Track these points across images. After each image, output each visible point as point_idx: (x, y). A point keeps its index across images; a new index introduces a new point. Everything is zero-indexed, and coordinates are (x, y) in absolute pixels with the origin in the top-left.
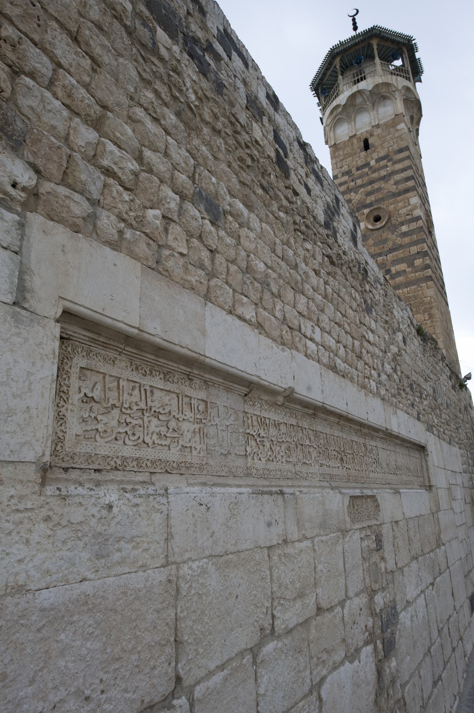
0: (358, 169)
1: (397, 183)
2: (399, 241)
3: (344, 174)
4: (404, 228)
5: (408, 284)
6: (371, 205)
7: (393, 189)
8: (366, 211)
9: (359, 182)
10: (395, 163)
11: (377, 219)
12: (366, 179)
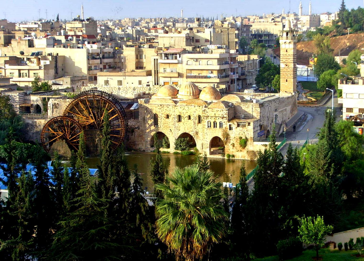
2: (289, 71)
4: (290, 69)
8: (285, 63)
9: (285, 58)
11: (287, 65)
12: (286, 58)
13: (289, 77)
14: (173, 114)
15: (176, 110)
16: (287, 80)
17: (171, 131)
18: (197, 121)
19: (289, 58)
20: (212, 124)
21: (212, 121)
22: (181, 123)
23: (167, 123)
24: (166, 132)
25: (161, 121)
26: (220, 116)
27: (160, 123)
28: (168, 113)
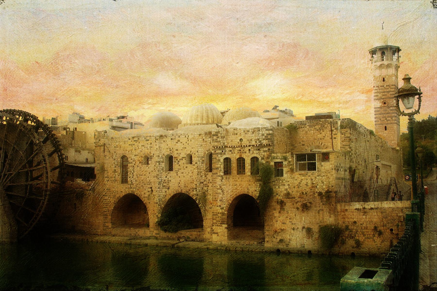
0: (381, 86)
1: (391, 95)
2: (390, 111)
3: (377, 87)
4: (391, 108)
5: (391, 123)
6: (383, 99)
7: (390, 96)
8: (382, 100)
10: (391, 88)
11: (385, 103)
13: (389, 122)
14: (157, 153)
15: (163, 146)
16: (386, 127)
17: (152, 191)
18: (204, 167)
19: (388, 90)
20: (234, 165)
21: (234, 157)
22: (172, 173)
23: (145, 173)
24: (143, 193)
25: (136, 172)
26: (253, 143)
27: (131, 176)
28: (146, 151)
